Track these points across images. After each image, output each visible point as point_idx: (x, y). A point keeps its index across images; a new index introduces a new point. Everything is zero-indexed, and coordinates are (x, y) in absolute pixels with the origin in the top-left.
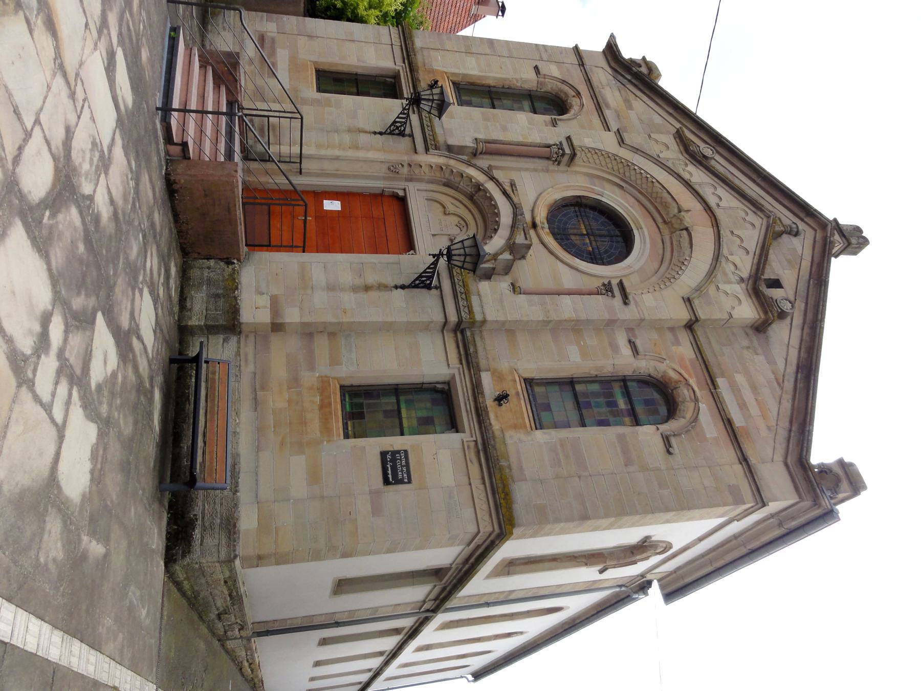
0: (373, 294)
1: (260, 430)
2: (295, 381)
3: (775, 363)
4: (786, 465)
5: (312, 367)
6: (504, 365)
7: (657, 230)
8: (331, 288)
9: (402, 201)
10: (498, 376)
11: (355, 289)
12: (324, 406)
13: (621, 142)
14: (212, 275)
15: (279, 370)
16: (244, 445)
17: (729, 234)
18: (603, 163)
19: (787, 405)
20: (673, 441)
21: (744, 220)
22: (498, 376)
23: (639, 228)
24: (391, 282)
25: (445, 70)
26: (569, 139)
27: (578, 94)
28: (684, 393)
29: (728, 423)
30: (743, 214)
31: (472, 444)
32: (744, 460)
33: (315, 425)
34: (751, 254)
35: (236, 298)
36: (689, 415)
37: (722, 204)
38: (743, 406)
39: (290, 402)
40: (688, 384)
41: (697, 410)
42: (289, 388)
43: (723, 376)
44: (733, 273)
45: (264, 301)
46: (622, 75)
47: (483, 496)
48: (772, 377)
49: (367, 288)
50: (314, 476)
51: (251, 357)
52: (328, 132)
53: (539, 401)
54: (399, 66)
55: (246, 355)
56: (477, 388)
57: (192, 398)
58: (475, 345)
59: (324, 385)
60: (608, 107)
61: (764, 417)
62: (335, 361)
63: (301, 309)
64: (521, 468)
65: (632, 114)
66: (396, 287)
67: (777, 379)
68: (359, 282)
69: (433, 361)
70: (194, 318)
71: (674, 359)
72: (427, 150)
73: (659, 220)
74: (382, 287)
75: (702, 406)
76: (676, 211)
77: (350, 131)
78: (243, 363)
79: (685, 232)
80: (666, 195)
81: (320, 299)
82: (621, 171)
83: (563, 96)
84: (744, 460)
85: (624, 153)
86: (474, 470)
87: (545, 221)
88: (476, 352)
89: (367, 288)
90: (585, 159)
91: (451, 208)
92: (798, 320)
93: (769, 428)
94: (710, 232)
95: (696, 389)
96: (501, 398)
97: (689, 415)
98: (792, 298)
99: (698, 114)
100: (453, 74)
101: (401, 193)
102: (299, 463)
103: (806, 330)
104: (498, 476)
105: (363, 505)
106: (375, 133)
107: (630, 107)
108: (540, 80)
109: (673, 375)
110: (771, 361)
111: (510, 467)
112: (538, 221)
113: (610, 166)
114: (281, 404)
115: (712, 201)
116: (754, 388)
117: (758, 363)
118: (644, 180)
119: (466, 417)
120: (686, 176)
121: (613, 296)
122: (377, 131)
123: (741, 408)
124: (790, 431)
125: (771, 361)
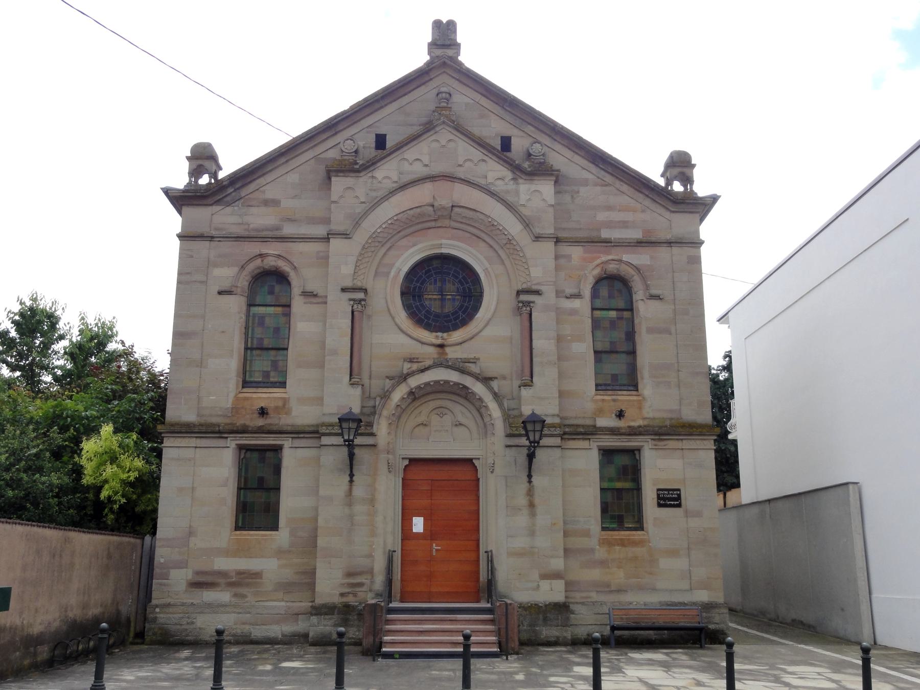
0: (537, 501)
1: (641, 588)
2: (603, 563)
3: (587, 180)
4: (673, 212)
5: (592, 550)
6: (590, 407)
7: (442, 230)
8: (532, 533)
9: (413, 461)
10: (600, 412)
11: (533, 514)
12: (622, 543)
13: (345, 235)
14: (525, 624)
15: (595, 574)
16: (653, 599)
17: (461, 169)
18: (367, 260)
19: (625, 188)
20: (654, 292)
21: (443, 146)
22: (600, 412)
23: (440, 246)
24: (524, 486)
25: (232, 395)
26: (344, 290)
27: (261, 256)
28: (612, 268)
29: (640, 243)
30: (434, 145)
31: (654, 442)
32: (670, 243)
33: (639, 551)
34: (485, 158)
35: (546, 606)
36: (632, 272)
37: (426, 160)
38: (624, 225)
39: (619, 567)
40: (607, 262)
41: (629, 264)
42: (608, 567)
43: (599, 230)
44: (506, 184)
45: (545, 585)
46: (226, 196)
47: (692, 442)
48: (599, 188)
49: (532, 505)
50: (673, 553)
51: (584, 595)
52: (352, 525)
53: (609, 382)
54: (232, 442)
55: (582, 598)
56: (613, 431)
57: (633, 632)
58: (578, 426)
59: (603, 542)
60: (278, 228)
61: (634, 211)
62: (587, 534)
63: (552, 557)
64: (671, 411)
65: (285, 203)
66: (530, 482)
67: (602, 186)
68: (525, 512)
69: (585, 460)
70: (565, 634)
71: (586, 267)
72: (372, 435)
73: (433, 224)
74: (530, 493)
75: (625, 258)
76: (431, 208)
77: (350, 504)
78: (589, 600)
79: (456, 210)
80: (411, 212)
81: (542, 542)
82: (377, 244)
83: (259, 271)
84: (670, 243)
85: (361, 237)
86: (672, 444)
87: (434, 334)
88: (583, 426)
89: (532, 505)
90: (362, 277)
91: (422, 418)
92: (456, 85)
93: (643, 211)
94: (459, 187)
95: (610, 257)
96: (620, 415)
97: (632, 272)
98: (531, 140)
99: (295, 135)
100: (237, 388)
101: (407, 462)
102: (665, 563)
103: (558, 138)
104: (681, 430)
105: (694, 523)
106: (351, 481)
107: (275, 203)
108: (239, 290)
109: (597, 271)
110: (585, 183)
111: (671, 419)
112: (439, 342)
113: (370, 254)
114: (621, 574)
115: (419, 170)
116: (609, 208)
117: (585, 192)
118: (391, 226)
119: (632, 443)
120: (389, 185)
121: (533, 302)
122: (348, 479)
123: (627, 227)
124: (647, 196)
125: (585, 183)
